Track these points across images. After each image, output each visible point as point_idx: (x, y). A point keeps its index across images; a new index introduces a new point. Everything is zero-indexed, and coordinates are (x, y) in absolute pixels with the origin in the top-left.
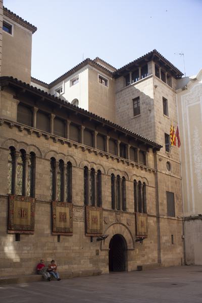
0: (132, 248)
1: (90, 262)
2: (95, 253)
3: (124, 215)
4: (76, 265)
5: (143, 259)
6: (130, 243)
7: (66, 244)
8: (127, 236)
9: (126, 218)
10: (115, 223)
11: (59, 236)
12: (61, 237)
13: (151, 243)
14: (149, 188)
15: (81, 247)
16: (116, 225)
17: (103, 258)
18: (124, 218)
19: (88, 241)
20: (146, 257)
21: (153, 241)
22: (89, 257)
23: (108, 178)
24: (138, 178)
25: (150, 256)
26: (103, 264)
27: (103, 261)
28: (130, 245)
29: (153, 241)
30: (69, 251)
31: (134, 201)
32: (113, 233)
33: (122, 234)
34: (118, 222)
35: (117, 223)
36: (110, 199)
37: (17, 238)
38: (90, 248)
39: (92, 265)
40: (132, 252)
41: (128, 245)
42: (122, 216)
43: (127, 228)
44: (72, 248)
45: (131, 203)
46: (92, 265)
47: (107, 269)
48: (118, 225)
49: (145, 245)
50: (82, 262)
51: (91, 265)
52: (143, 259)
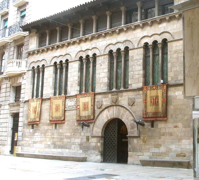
0: (136, 134)
1: (81, 148)
2: (85, 140)
3: (124, 94)
4: (68, 150)
5: (156, 150)
6: (132, 128)
7: (61, 131)
8: (127, 119)
9: (126, 98)
10: (110, 106)
11: (56, 124)
12: (57, 125)
13: (176, 127)
14: (174, 44)
15: (72, 134)
16: (112, 108)
17: (94, 144)
18: (124, 99)
19: (79, 128)
20: (162, 149)
21: (180, 125)
22: (79, 143)
23: (104, 59)
24: (152, 38)
25: (173, 147)
26: (93, 151)
27: (94, 148)
28: (132, 131)
29: (180, 125)
30: (62, 137)
31: (141, 72)
32: (107, 117)
33: (120, 118)
34: (115, 104)
35: (113, 106)
36: (106, 80)
37: (33, 128)
38: (81, 134)
39: (81, 151)
40: (135, 141)
41: (129, 130)
42: (122, 96)
43: (126, 109)
44: (65, 135)
45: (137, 76)
46: (81, 151)
47: (99, 157)
48: (115, 107)
49: (163, 131)
50: (73, 146)
51: (81, 151)
52: (156, 150)
